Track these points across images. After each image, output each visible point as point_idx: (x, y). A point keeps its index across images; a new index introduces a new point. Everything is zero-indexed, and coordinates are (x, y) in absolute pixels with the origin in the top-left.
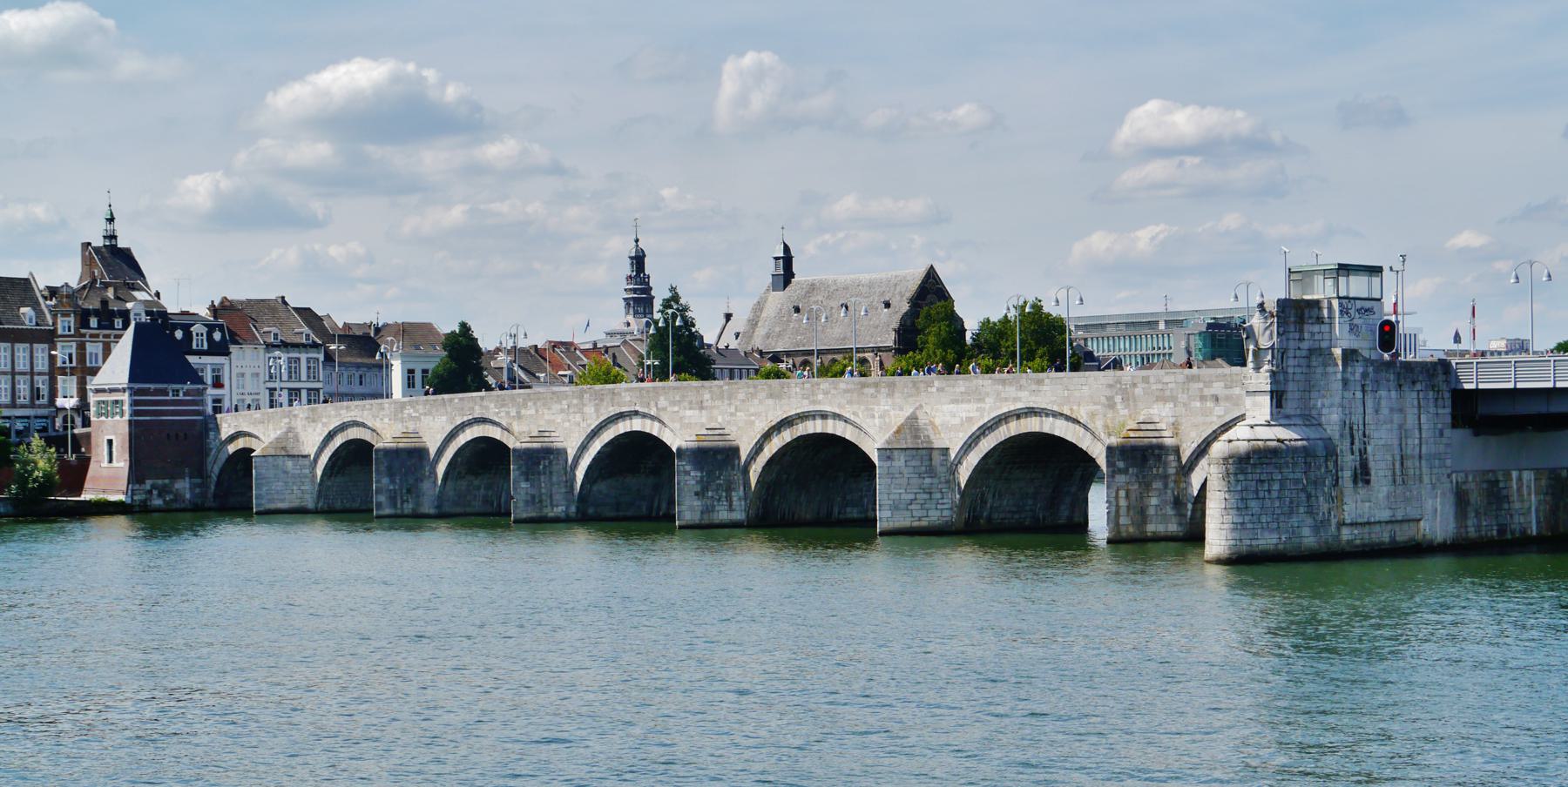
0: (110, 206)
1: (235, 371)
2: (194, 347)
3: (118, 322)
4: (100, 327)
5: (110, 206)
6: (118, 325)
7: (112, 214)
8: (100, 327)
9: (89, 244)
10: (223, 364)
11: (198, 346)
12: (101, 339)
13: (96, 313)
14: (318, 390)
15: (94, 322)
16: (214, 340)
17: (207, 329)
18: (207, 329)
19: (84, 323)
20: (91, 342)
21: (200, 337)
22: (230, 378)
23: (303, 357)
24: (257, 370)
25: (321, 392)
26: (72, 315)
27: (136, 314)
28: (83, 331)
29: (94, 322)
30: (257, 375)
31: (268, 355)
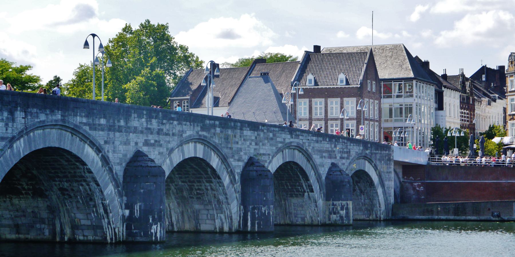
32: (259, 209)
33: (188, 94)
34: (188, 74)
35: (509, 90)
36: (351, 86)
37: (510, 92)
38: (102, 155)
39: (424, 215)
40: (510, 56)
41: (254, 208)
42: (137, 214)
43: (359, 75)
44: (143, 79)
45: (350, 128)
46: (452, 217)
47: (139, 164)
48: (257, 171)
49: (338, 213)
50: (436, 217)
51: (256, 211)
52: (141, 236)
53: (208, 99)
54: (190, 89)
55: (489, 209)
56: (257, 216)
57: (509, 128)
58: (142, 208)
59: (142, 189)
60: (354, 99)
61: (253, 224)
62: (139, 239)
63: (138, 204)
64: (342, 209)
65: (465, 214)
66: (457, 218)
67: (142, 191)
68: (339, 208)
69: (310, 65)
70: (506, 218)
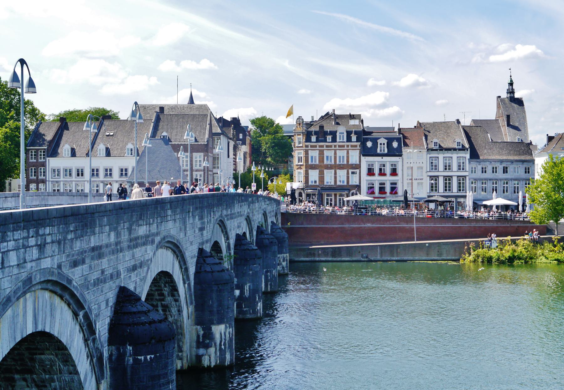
0: (511, 76)
1: (406, 166)
2: (378, 151)
3: (329, 138)
4: (317, 141)
5: (511, 76)
6: (329, 140)
7: (511, 81)
8: (317, 141)
9: (500, 97)
10: (398, 161)
11: (381, 151)
12: (318, 148)
13: (316, 133)
14: (465, 176)
15: (314, 138)
16: (393, 147)
17: (387, 141)
18: (387, 141)
19: (308, 140)
20: (312, 150)
21: (382, 146)
22: (403, 170)
23: (455, 156)
24: (421, 165)
25: (467, 178)
26: (302, 135)
27: (340, 133)
28: (307, 144)
29: (314, 138)
30: (422, 168)
31: (429, 156)
32: (271, 272)
33: (44, 144)
34: (38, 126)
35: (297, 145)
36: (199, 143)
37: (297, 147)
38: (228, 243)
39: (307, 257)
40: (298, 119)
41: (267, 272)
42: (247, 294)
43: (204, 134)
44: (8, 130)
45: (198, 178)
46: (330, 259)
47: (246, 247)
48: (268, 239)
49: (281, 264)
50: (317, 259)
51: (269, 274)
52: (250, 314)
53: (65, 148)
54: (44, 140)
55: (360, 252)
56: (269, 278)
57: (296, 175)
58: (251, 288)
59: (251, 270)
60: (202, 154)
61: (266, 285)
62: (249, 316)
63: (248, 285)
64: (284, 261)
65: (340, 256)
66: (335, 259)
67: (251, 272)
68: (282, 260)
69: (161, 124)
70: (372, 259)
